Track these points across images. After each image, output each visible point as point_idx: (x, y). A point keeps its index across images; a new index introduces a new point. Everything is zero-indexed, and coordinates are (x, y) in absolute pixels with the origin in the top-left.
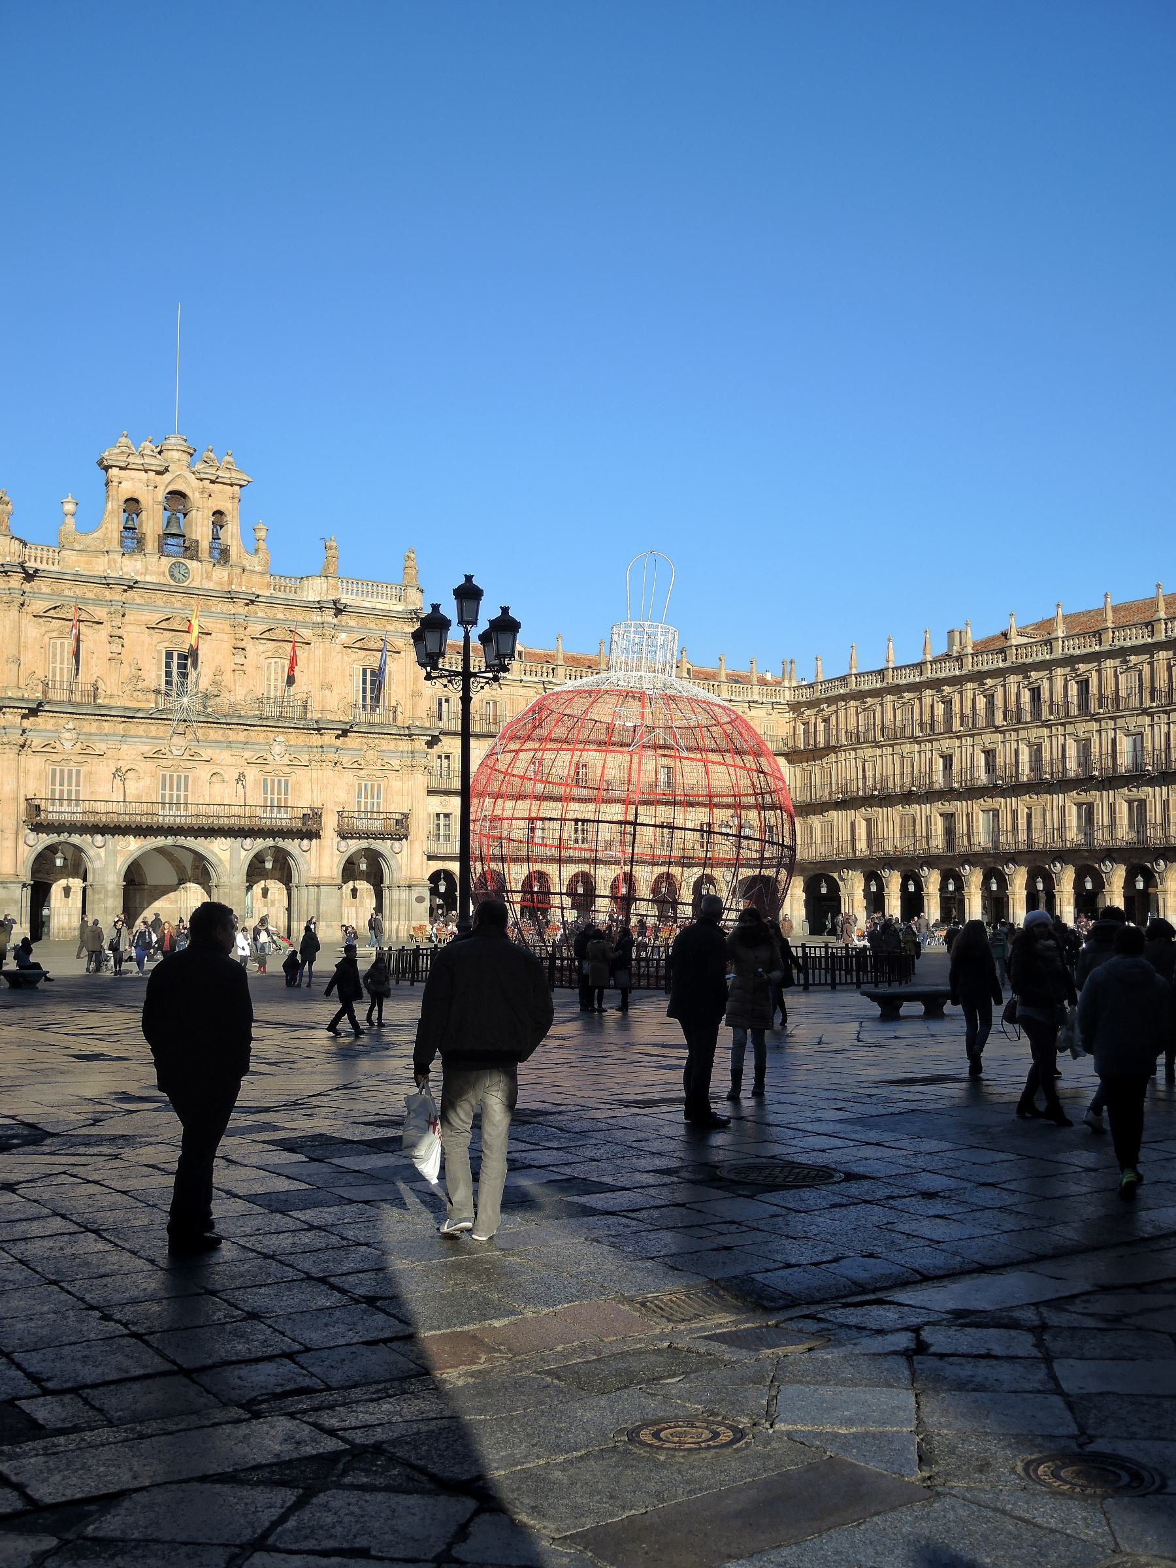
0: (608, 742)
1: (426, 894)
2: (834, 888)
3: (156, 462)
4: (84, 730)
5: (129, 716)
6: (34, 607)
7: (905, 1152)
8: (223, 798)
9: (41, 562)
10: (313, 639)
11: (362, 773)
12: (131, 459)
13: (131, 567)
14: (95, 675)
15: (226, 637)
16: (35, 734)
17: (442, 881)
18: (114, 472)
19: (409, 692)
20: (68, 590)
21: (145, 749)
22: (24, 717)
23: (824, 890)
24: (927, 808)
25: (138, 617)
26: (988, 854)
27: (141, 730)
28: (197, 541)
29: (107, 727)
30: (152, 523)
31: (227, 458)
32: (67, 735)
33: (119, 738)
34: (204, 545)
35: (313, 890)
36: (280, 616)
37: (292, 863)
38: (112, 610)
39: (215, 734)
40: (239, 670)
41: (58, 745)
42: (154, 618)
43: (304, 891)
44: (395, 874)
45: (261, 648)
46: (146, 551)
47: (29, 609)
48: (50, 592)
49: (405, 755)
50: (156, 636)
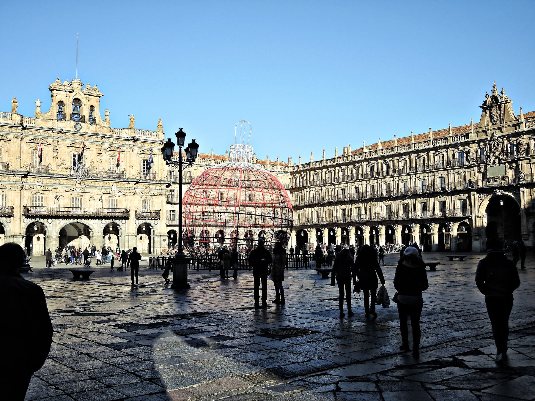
0: (230, 185)
1: (167, 238)
2: (306, 234)
3: (69, 88)
4: (44, 182)
5: (60, 177)
6: (26, 139)
7: (331, 323)
8: (94, 205)
9: (28, 123)
10: (126, 150)
11: (143, 197)
12: (61, 87)
13: (61, 125)
14: (48, 163)
15: (95, 149)
16: (27, 183)
17: (172, 234)
18: (54, 92)
19: (160, 169)
20: (38, 133)
21: (66, 189)
22: (23, 177)
23: (303, 235)
24: (336, 207)
25: (63, 143)
26: (357, 222)
27: (65, 182)
28: (84, 116)
29: (53, 181)
30: (68, 109)
31: (95, 87)
32: (38, 184)
33: (57, 185)
34: (87, 118)
35: (127, 238)
36: (114, 142)
37: (119, 228)
38: (54, 140)
39: (91, 183)
40: (100, 161)
41: (35, 187)
42: (69, 143)
43: (123, 238)
44: (156, 231)
45: (108, 153)
46: (66, 119)
47: (24, 140)
48: (32, 134)
49: (159, 190)
50: (70, 149)
